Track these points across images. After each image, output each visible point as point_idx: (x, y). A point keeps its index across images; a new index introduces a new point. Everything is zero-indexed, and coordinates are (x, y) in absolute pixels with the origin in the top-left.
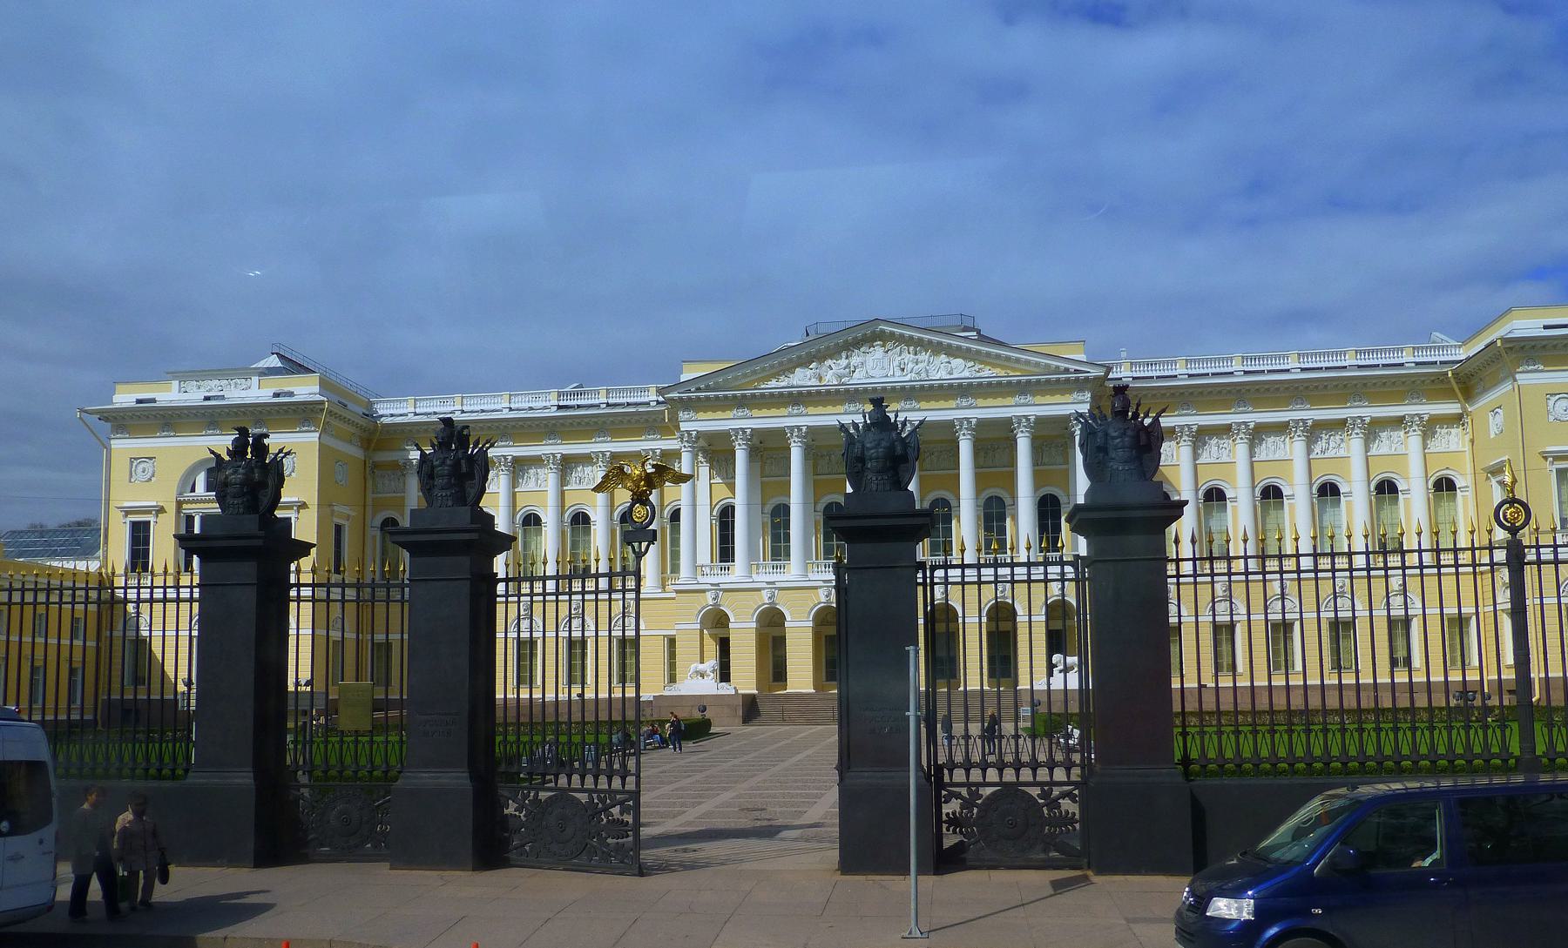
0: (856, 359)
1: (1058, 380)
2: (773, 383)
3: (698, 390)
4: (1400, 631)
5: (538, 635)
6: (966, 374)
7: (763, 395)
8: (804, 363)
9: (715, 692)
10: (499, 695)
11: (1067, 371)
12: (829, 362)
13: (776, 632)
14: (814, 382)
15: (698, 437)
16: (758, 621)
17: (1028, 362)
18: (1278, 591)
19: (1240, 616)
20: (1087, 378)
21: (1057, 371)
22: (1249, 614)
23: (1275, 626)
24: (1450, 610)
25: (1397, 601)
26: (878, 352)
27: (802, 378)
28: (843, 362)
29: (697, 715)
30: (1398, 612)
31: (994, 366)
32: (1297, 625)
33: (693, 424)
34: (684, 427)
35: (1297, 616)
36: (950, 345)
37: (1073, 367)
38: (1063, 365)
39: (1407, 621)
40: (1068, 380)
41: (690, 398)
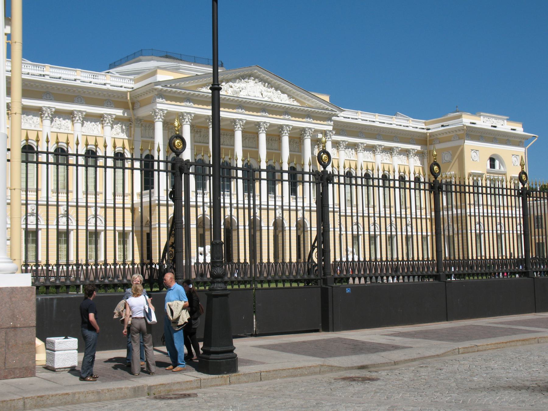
3: (171, 87)
4: (63, 238)
5: (101, 227)
6: (288, 102)
10: (332, 259)
11: (327, 109)
12: (231, 84)
18: (94, 213)
19: (72, 226)
21: (323, 109)
22: (47, 225)
23: (91, 233)
24: (91, 228)
25: (63, 220)
26: (251, 82)
30: (63, 227)
31: (298, 101)
32: (103, 234)
33: (163, 106)
35: (103, 228)
39: (67, 233)
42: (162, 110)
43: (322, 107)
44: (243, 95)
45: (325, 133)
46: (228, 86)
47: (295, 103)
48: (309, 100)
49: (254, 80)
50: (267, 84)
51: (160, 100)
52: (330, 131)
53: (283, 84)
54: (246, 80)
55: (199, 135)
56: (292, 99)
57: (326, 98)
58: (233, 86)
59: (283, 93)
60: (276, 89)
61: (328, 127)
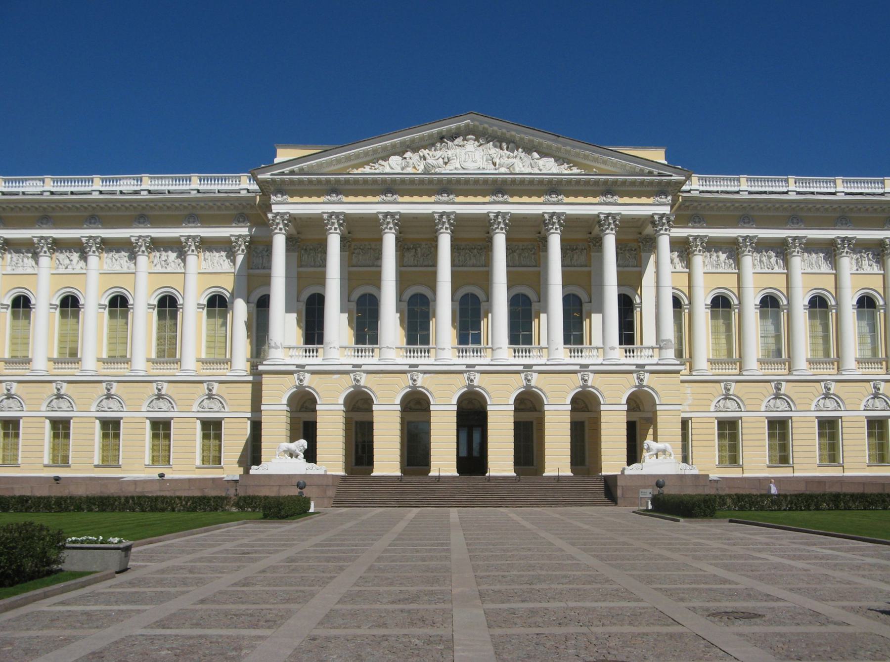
0: (450, 153)
1: (642, 183)
2: (367, 169)
6: (555, 172)
7: (356, 182)
8: (401, 153)
9: (303, 472)
12: (423, 152)
13: (359, 417)
14: (410, 170)
15: (289, 221)
16: (345, 404)
17: (614, 165)
20: (669, 183)
26: (471, 145)
27: (394, 165)
28: (438, 154)
29: (295, 492)
33: (284, 206)
34: (275, 209)
36: (540, 144)
37: (656, 171)
38: (647, 169)
40: (651, 183)
41: (283, 181)
42: (282, 215)
43: (637, 170)
44: (448, 169)
45: (651, 220)
46: (418, 158)
47: (575, 170)
48: (605, 162)
49: (477, 140)
50: (504, 145)
51: (279, 198)
52: (662, 216)
53: (539, 138)
54: (459, 141)
55: (412, 254)
56: (566, 165)
57: (658, 155)
58: (427, 156)
59: (543, 155)
60: (528, 150)
61: (660, 208)
